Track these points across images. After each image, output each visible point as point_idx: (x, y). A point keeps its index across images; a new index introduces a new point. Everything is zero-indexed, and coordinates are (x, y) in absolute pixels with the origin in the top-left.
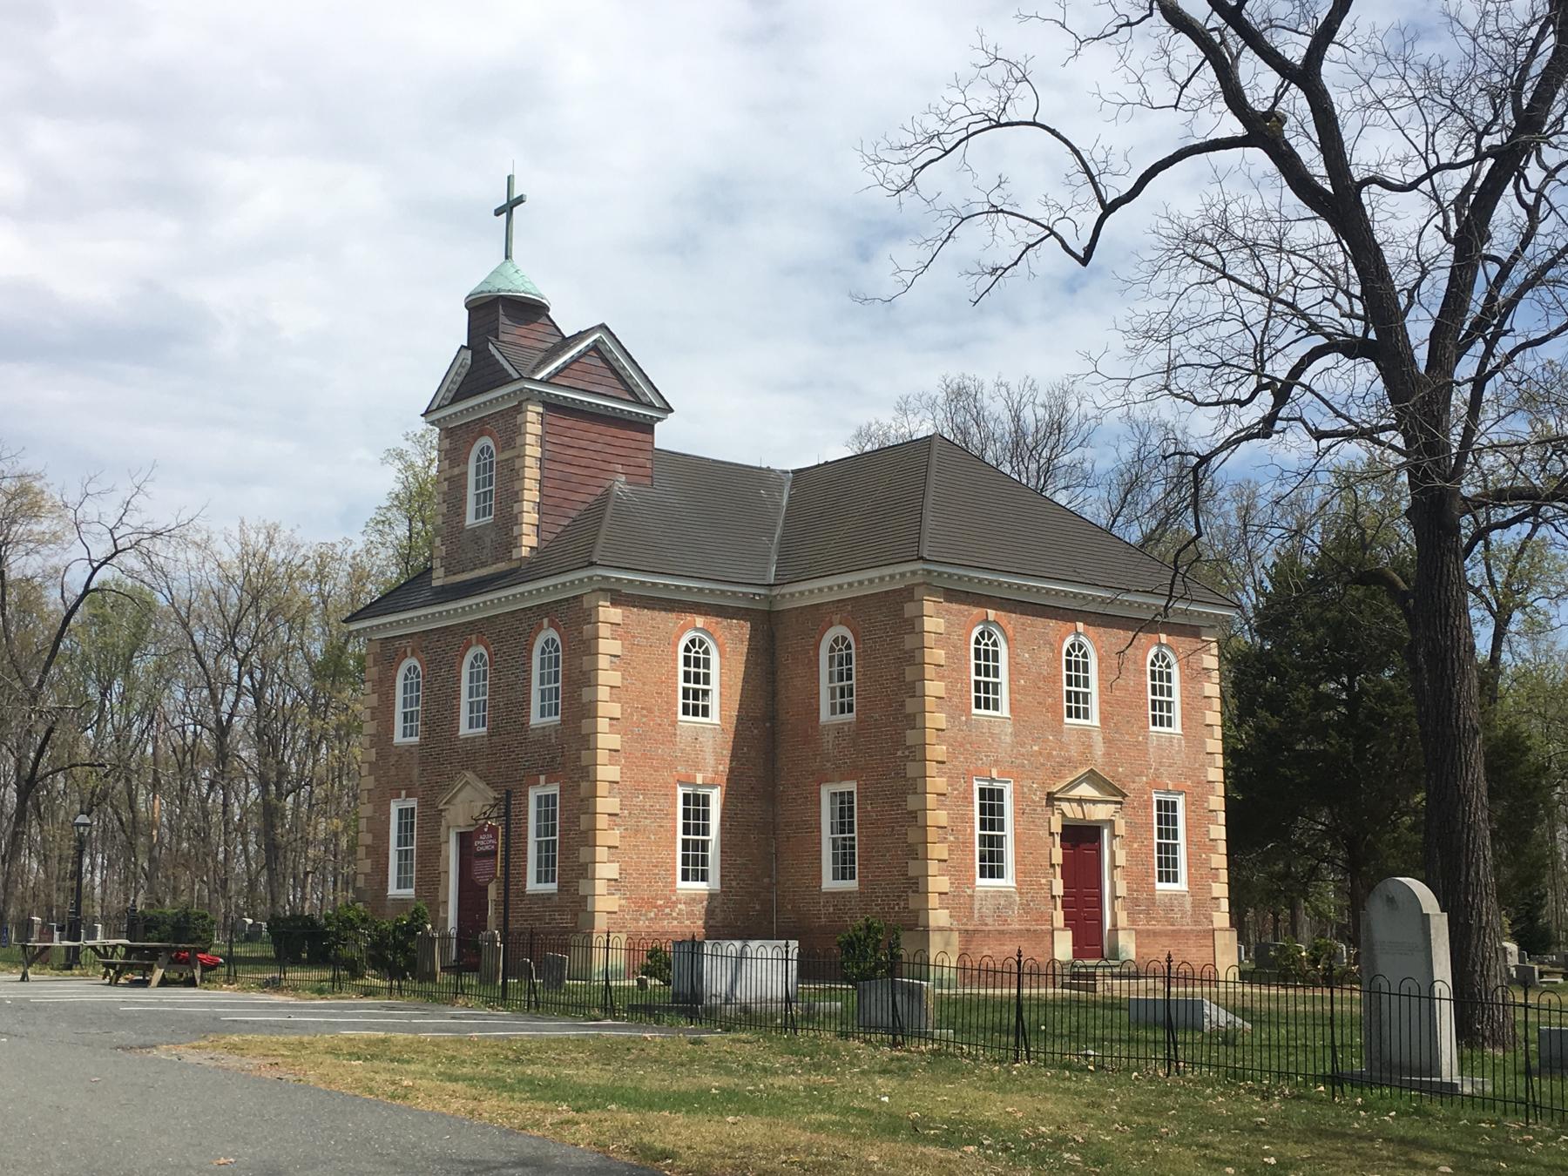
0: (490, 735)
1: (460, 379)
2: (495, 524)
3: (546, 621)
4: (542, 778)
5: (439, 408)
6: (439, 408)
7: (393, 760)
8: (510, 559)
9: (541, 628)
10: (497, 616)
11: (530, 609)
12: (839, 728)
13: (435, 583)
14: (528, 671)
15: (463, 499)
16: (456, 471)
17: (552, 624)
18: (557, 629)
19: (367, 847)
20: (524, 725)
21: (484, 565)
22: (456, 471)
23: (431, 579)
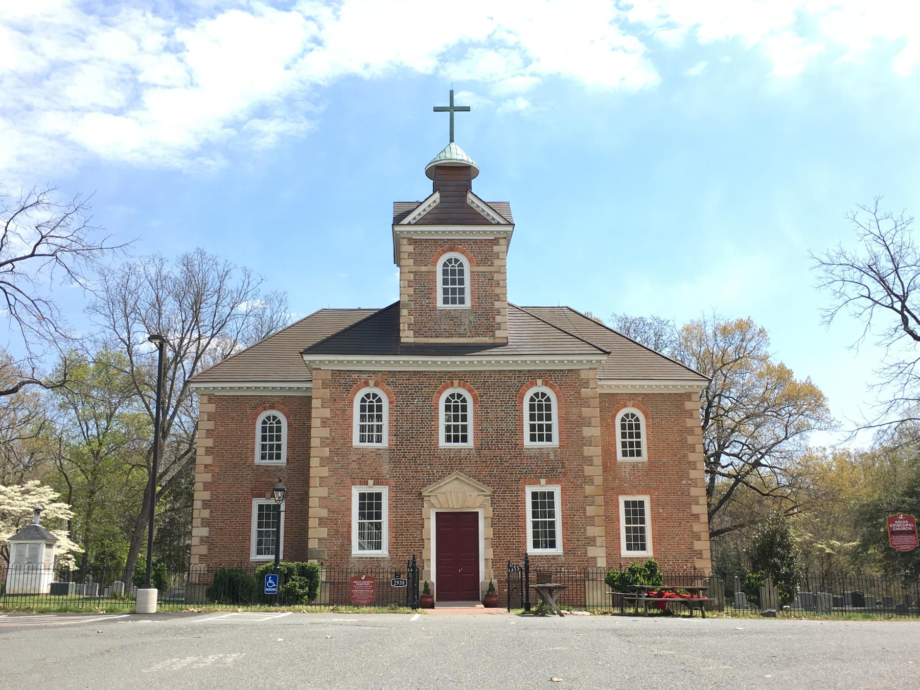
1: (430, 209)
2: (473, 311)
3: (539, 382)
5: (409, 224)
6: (409, 224)
8: (493, 336)
9: (534, 384)
10: (481, 372)
11: (520, 371)
12: (634, 466)
13: (403, 340)
15: (433, 290)
16: (423, 269)
17: (546, 383)
18: (552, 387)
19: (320, 519)
20: (518, 445)
21: (461, 335)
22: (423, 269)
23: (399, 338)
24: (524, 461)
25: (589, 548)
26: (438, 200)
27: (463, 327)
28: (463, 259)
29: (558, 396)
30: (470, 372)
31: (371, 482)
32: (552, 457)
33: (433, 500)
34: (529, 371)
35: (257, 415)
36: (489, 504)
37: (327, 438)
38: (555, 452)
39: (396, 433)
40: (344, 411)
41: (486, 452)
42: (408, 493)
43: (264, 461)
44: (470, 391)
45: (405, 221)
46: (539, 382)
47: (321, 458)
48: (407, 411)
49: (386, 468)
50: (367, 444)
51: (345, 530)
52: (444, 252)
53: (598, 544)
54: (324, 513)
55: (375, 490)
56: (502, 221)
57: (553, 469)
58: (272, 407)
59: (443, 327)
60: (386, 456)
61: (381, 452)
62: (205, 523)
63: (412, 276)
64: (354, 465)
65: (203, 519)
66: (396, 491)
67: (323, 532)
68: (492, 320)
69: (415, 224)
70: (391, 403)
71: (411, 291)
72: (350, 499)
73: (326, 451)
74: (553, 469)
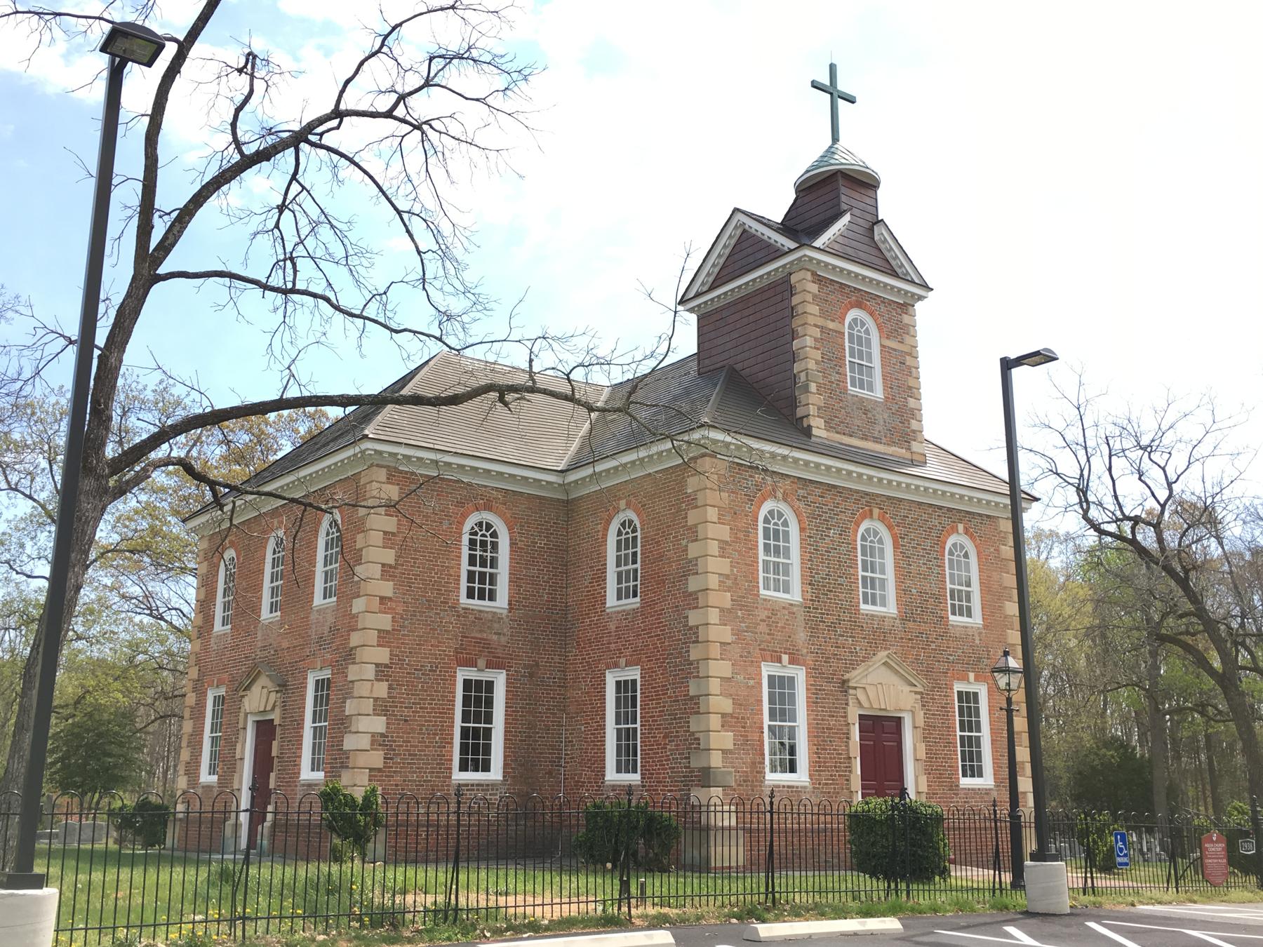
4: (972, 676)
8: (909, 449)
11: (940, 508)
18: (972, 537)
19: (724, 715)
22: (831, 325)
27: (877, 428)
28: (870, 323)
30: (889, 498)
32: (977, 642)
33: (861, 695)
34: (949, 509)
35: (465, 517)
36: (918, 706)
37: (727, 576)
39: (810, 581)
40: (747, 534)
41: (911, 624)
43: (471, 601)
44: (890, 528)
46: (961, 527)
47: (722, 610)
49: (801, 636)
54: (726, 705)
58: (488, 507)
61: (795, 609)
62: (381, 708)
64: (763, 628)
65: (376, 699)
66: (815, 675)
70: (802, 530)
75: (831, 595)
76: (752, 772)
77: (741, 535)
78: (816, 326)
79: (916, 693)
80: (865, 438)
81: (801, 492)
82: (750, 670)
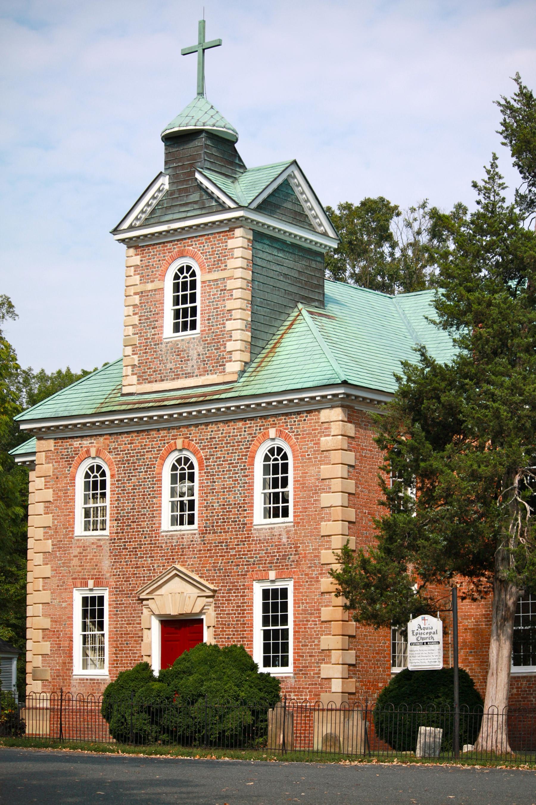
0: (203, 533)
5: (131, 228)
6: (131, 228)
7: (75, 551)
14: (251, 477)
15: (159, 314)
16: (150, 286)
18: (287, 438)
20: (246, 526)
21: (188, 375)
22: (150, 286)
24: (253, 547)
25: (322, 666)
26: (167, 187)
27: (190, 363)
29: (293, 451)
31: (91, 583)
32: (284, 540)
38: (288, 532)
41: (210, 537)
42: (128, 596)
45: (125, 225)
48: (129, 487)
49: (106, 564)
50: (91, 533)
51: (66, 644)
52: (174, 259)
53: (333, 661)
54: (46, 623)
55: (97, 593)
56: (232, 205)
57: (284, 557)
59: (169, 366)
60: (106, 548)
61: (102, 543)
63: (136, 300)
64: (75, 562)
67: (46, 647)
68: (222, 348)
69: (141, 227)
71: (136, 320)
72: (71, 605)
73: (48, 545)
74: (284, 557)
75: (134, 525)
76: (62, 669)
77: (61, 494)
78: (136, 294)
79: (207, 597)
80: (177, 377)
81: (113, 445)
82: (63, 595)
